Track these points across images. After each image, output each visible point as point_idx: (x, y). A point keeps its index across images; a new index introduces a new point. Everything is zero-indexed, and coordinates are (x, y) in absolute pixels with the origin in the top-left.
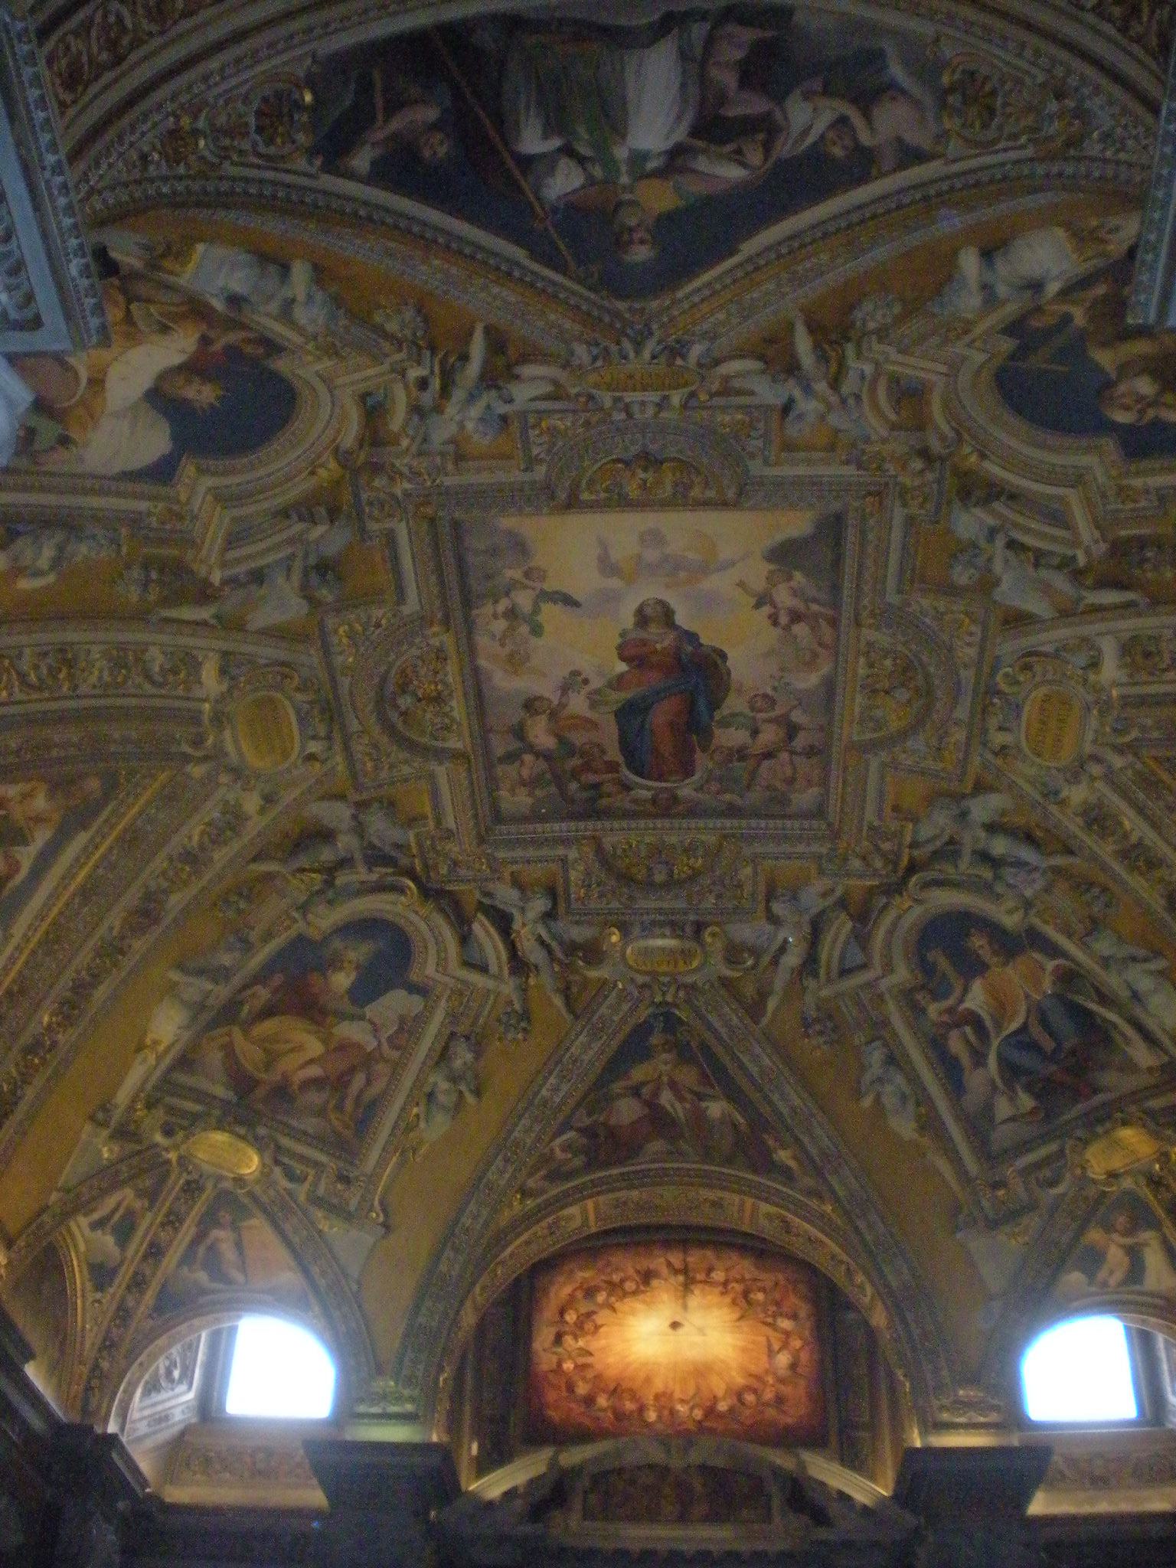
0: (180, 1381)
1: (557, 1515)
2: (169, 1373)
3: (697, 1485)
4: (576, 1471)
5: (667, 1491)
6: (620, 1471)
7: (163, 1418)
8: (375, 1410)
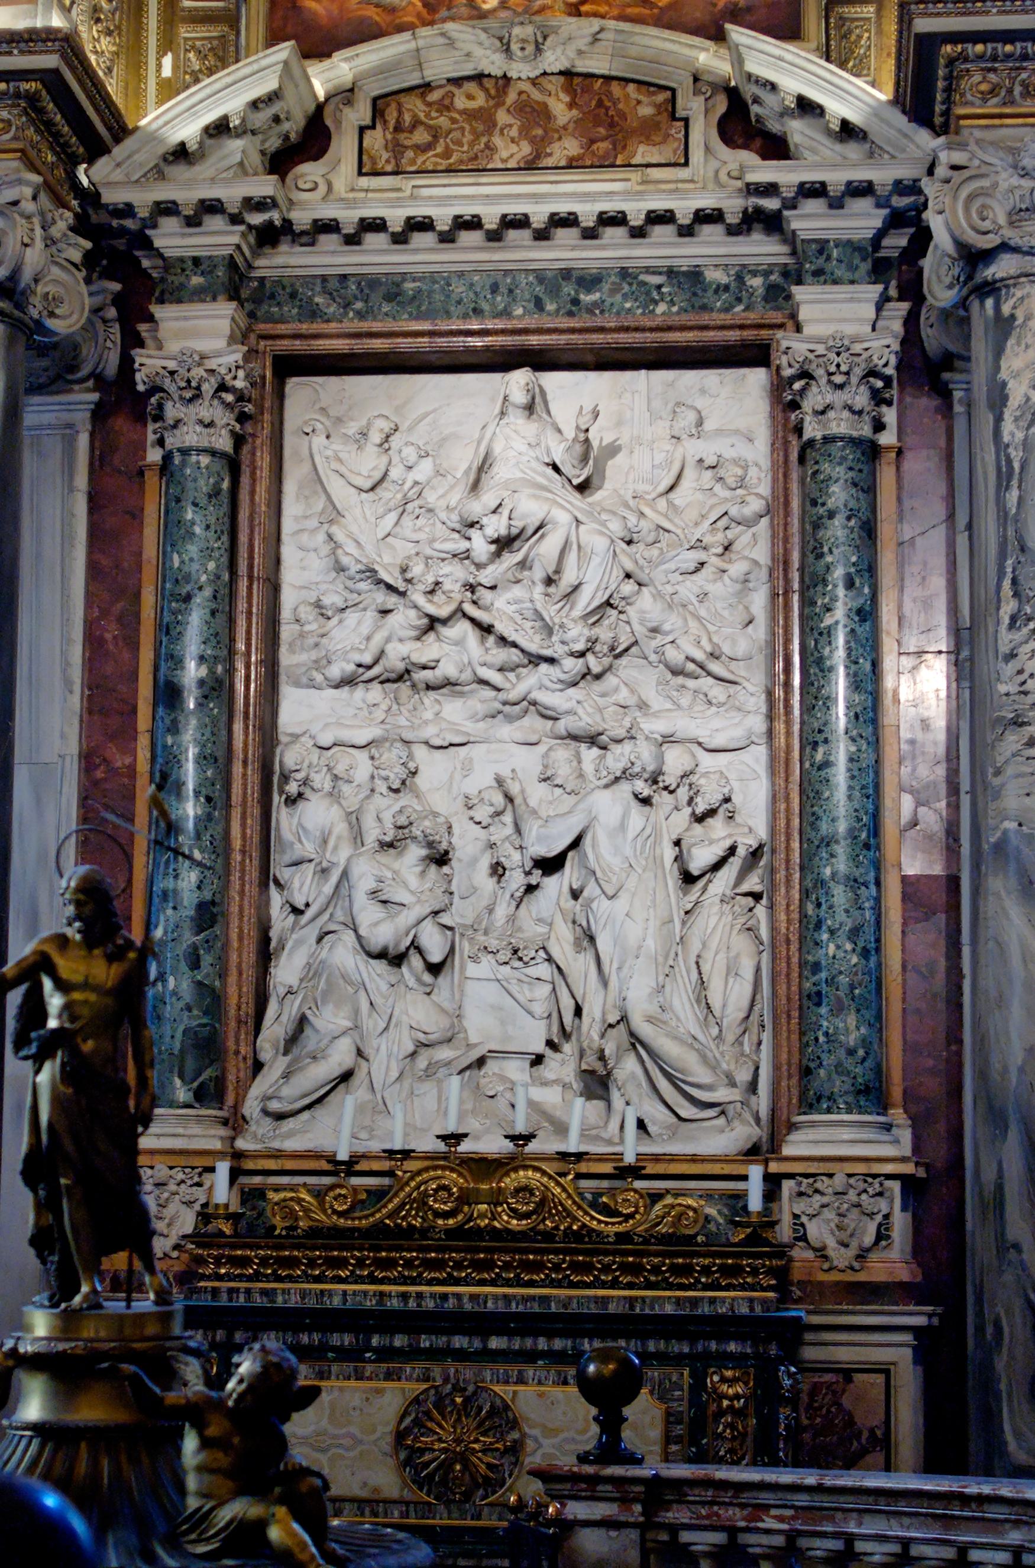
1: (309, 171)
3: (560, 109)
4: (347, 94)
5: (502, 117)
6: (426, 87)
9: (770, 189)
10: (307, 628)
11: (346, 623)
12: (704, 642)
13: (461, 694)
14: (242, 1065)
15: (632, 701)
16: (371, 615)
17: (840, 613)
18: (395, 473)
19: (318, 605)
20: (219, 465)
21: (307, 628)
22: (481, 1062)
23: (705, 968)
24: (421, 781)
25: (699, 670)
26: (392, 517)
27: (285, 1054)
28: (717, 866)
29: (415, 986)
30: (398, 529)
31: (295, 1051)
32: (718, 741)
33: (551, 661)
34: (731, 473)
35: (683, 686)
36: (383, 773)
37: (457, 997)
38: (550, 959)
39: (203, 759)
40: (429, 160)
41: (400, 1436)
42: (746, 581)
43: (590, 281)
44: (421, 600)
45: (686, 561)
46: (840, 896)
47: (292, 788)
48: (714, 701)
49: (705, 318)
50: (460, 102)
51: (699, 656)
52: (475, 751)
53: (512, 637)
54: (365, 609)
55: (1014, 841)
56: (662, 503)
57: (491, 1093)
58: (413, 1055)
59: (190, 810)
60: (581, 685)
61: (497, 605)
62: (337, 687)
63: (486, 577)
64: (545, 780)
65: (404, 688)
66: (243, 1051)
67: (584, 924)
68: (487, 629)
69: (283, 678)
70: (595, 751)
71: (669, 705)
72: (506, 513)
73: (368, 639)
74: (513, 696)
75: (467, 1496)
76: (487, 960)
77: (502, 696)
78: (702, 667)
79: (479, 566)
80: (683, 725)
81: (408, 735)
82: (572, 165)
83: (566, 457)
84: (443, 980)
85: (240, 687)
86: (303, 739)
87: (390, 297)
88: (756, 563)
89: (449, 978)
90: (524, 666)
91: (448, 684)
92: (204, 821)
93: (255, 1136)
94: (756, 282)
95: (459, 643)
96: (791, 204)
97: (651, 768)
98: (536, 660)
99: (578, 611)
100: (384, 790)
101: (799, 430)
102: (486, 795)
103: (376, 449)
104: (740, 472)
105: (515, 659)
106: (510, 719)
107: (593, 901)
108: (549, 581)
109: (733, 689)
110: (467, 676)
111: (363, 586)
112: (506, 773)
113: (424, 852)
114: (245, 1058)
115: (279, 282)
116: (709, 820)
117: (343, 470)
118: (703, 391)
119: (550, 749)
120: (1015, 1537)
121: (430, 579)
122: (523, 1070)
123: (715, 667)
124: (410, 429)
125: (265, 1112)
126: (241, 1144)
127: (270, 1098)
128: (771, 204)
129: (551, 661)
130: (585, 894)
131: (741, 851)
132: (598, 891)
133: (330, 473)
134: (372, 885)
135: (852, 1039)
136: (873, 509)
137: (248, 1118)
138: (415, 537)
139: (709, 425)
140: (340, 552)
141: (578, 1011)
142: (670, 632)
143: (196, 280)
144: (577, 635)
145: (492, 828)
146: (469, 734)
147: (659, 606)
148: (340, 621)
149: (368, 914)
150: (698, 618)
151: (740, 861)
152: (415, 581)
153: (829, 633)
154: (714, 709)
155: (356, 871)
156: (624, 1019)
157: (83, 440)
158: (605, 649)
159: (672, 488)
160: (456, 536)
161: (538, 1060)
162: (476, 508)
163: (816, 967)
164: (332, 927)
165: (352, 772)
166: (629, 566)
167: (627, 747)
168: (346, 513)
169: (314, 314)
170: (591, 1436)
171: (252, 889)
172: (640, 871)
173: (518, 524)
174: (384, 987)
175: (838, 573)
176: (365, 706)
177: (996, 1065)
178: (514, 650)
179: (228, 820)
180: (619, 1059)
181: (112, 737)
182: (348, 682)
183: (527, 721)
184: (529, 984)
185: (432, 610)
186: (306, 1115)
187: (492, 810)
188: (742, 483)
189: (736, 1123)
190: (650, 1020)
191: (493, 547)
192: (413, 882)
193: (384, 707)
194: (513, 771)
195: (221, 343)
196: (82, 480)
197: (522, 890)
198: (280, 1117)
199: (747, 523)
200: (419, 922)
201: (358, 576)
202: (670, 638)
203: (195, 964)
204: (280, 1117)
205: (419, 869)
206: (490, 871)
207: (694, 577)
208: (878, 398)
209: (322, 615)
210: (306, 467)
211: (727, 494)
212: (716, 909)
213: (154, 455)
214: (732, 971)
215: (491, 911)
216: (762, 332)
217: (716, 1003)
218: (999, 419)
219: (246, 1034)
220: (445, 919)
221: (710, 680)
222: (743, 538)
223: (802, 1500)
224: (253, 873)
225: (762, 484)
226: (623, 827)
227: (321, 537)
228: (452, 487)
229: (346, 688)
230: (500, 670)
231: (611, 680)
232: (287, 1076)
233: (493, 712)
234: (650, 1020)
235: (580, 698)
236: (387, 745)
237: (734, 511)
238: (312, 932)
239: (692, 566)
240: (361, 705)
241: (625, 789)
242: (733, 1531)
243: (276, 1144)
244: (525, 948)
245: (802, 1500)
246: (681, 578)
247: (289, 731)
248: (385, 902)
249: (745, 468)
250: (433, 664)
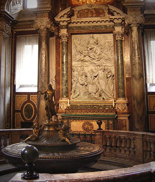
0: (19, 4)
2: (16, 3)
5: (89, 12)
7: (16, 9)
8: (42, 3)
9: (112, 18)
16: (80, 55)
17: (119, 55)
20: (66, 43)
22: (90, 94)
28: (110, 77)
34: (110, 43)
39: (65, 68)
40: (83, 16)
41: (83, 126)
43: (97, 26)
44: (84, 54)
46: (120, 79)
47: (73, 70)
49: (107, 30)
50: (86, 11)
51: (108, 58)
53: (92, 57)
55: (135, 75)
59: (65, 72)
63: (89, 52)
65: (83, 61)
68: (90, 57)
69: (72, 61)
74: (92, 62)
75: (89, 131)
76: (90, 85)
80: (107, 64)
82: (95, 16)
85: (69, 62)
87: (80, 28)
92: (66, 73)
94: (111, 26)
96: (114, 20)
97: (104, 68)
98: (94, 59)
99: (97, 55)
101: (115, 39)
110: (88, 60)
112: (92, 69)
115: (71, 27)
118: (107, 35)
120: (134, 136)
123: (109, 59)
128: (112, 20)
131: (112, 75)
134: (80, 79)
135: (122, 92)
136: (122, 46)
139: (108, 38)
141: (98, 89)
143: (64, 27)
144: (97, 57)
149: (80, 81)
153: (119, 57)
155: (79, 77)
157: (55, 41)
161: (95, 93)
162: (88, 46)
163: (119, 85)
167: (102, 67)
169: (74, 30)
170: (98, 127)
171: (70, 79)
175: (119, 51)
177: (134, 94)
179: (68, 73)
181: (58, 66)
182: (78, 61)
190: (104, 90)
195: (66, 32)
196: (55, 44)
198: (73, 98)
199: (112, 47)
203: (66, 86)
204: (73, 98)
208: (122, 36)
213: (61, 42)
214: (111, 85)
215: (91, 80)
217: (110, 88)
218: (132, 38)
220: (87, 81)
223: (116, 133)
224: (70, 78)
225: (113, 43)
226: (102, 73)
232: (74, 95)
234: (104, 90)
241: (102, 70)
242: (110, 136)
245: (116, 133)
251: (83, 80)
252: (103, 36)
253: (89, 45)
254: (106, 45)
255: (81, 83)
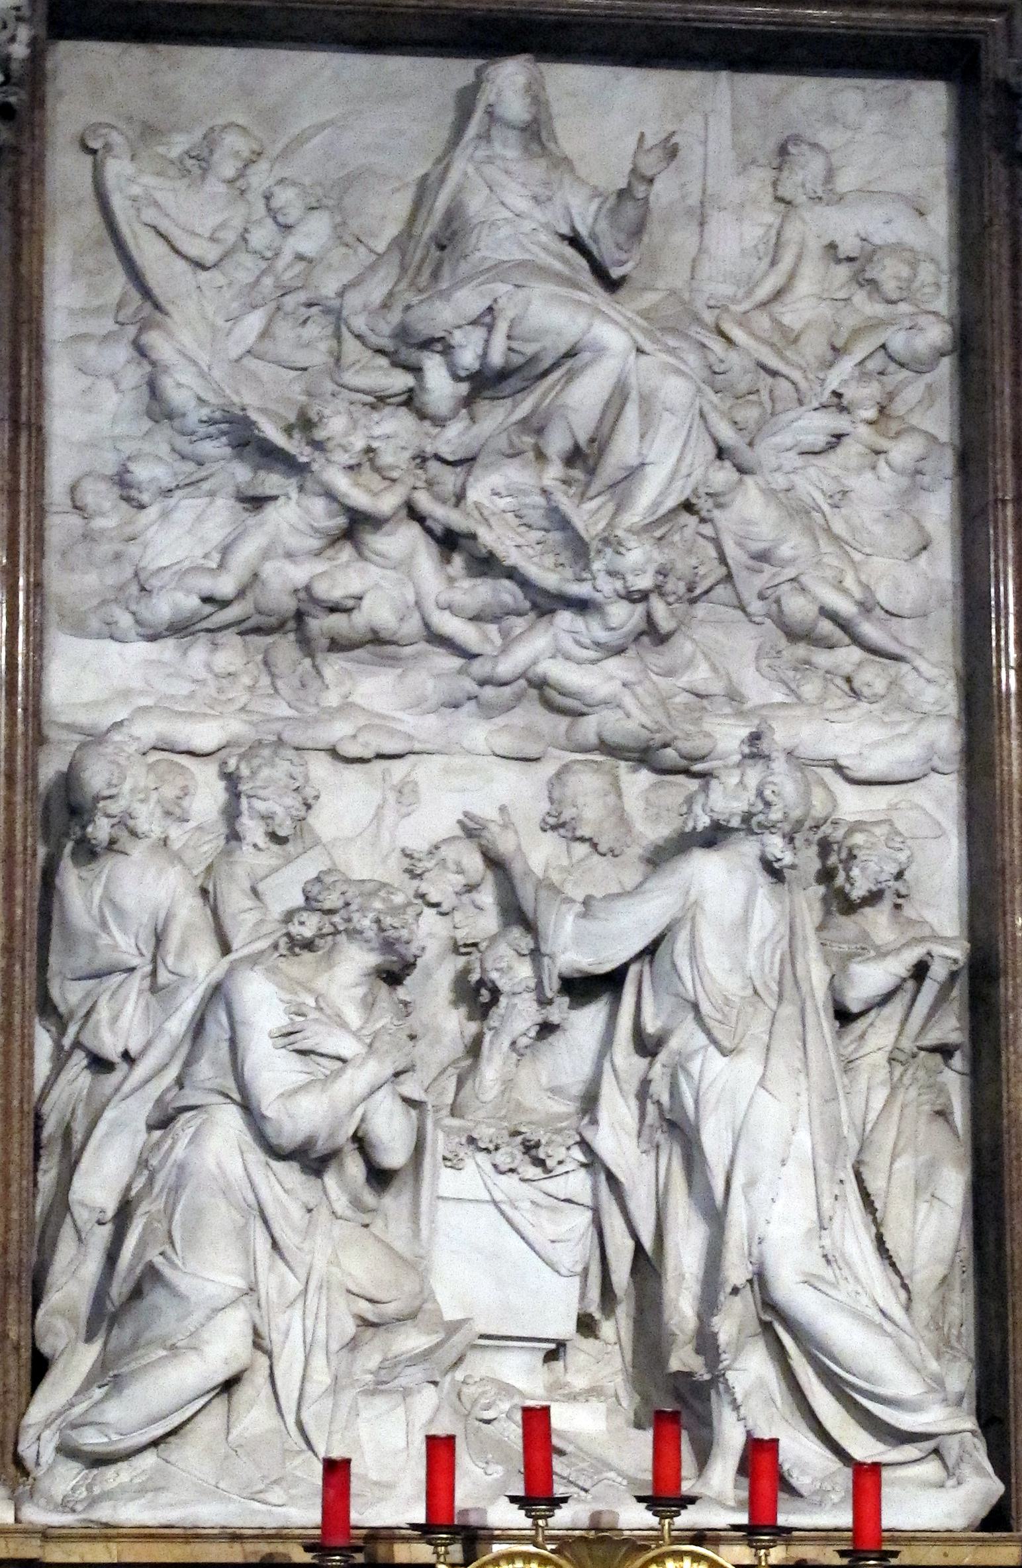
10: (99, 523)
11: (177, 516)
12: (849, 582)
13: (394, 661)
14: (11, 1361)
15: (717, 687)
18: (261, 236)
19: (123, 482)
21: (99, 523)
23: (875, 1185)
24: (323, 822)
25: (838, 634)
26: (254, 322)
27: (89, 1339)
29: (349, 1213)
30: (268, 345)
31: (123, 1335)
32: (874, 766)
33: (582, 606)
34: (889, 273)
35: (807, 662)
36: (260, 806)
37: (425, 1233)
38: (593, 1162)
42: (919, 472)
44: (342, 483)
45: (806, 431)
48: (866, 691)
51: (845, 607)
52: (425, 771)
53: (512, 556)
54: (212, 494)
56: (762, 321)
57: (488, 1415)
58: (353, 1345)
60: (631, 653)
61: (473, 495)
62: (153, 638)
64: (554, 828)
66: (13, 1335)
67: (665, 1099)
70: (645, 777)
71: (778, 696)
72: (502, 328)
73: (226, 550)
74: (506, 667)
77: (479, 668)
78: (844, 625)
79: (440, 422)
81: (294, 736)
83: (603, 226)
84: (394, 1203)
86: (117, 737)
88: (933, 439)
89: (406, 1198)
90: (520, 614)
91: (376, 639)
93: (50, 1499)
95: (404, 566)
100: (262, 841)
102: (447, 852)
103: (222, 188)
104: (905, 271)
105: (507, 598)
106: (488, 711)
107: (690, 1057)
108: (574, 457)
109: (893, 667)
110: (413, 626)
111: (209, 448)
112: (487, 811)
113: (373, 959)
114: (17, 1348)
116: (867, 910)
117: (165, 225)
118: (832, 119)
119: (565, 769)
121: (359, 443)
122: (531, 1371)
123: (870, 630)
124: (286, 153)
125: (68, 1451)
126: (35, 1515)
127: (74, 1426)
129: (582, 606)
130: (674, 1043)
131: (939, 971)
132: (701, 1039)
133: (138, 227)
137: (29, 1463)
138: (301, 358)
139: (846, 181)
140: (167, 384)
142: (792, 561)
145: (458, 916)
146: (410, 737)
147: (773, 514)
148: (165, 515)
150: (836, 539)
151: (936, 987)
152: (330, 445)
154: (864, 706)
156: (760, 1280)
158: (682, 587)
159: (778, 294)
160: (383, 361)
161: (555, 1352)
164: (190, 1097)
165: (185, 803)
166: (727, 434)
168: (169, 308)
172: (773, 1004)
173: (530, 349)
174: (297, 1213)
176: (210, 676)
178: (507, 583)
180: (739, 1348)
182: (181, 628)
183: (518, 717)
184: (553, 1209)
185: (360, 499)
186: (149, 1460)
187: (460, 880)
188: (907, 292)
189: (966, 1470)
191: (464, 388)
192: (353, 1016)
193: (246, 680)
194: (503, 809)
197: (533, 1033)
198: (99, 1461)
199: (916, 365)
200: (373, 1092)
201: (203, 430)
202: (790, 572)
204: (99, 1461)
205: (360, 991)
206: (451, 996)
207: (820, 461)
209: (127, 499)
210: (90, 216)
211: (879, 309)
212: (883, 1074)
214: (923, 1187)
216: (967, 19)
219: (19, 1301)
221: (856, 653)
222: (913, 392)
224: (31, 993)
226: (745, 922)
227: (122, 353)
228: (372, 268)
229: (171, 642)
230: (476, 618)
231: (683, 647)
233: (460, 695)
234: (810, 1281)
235: (630, 676)
236: (266, 752)
237: (898, 342)
238: (139, 1109)
239: (821, 441)
240: (203, 674)
241: (749, 849)
243: (104, 1513)
244: (548, 1144)
246: (799, 461)
247: (64, 719)
248: (303, 1053)
249: (914, 265)
250: (350, 603)
251: (347, 1046)
252: (736, 107)
253: (470, 301)
254: (793, 314)
255: (290, 1130)
